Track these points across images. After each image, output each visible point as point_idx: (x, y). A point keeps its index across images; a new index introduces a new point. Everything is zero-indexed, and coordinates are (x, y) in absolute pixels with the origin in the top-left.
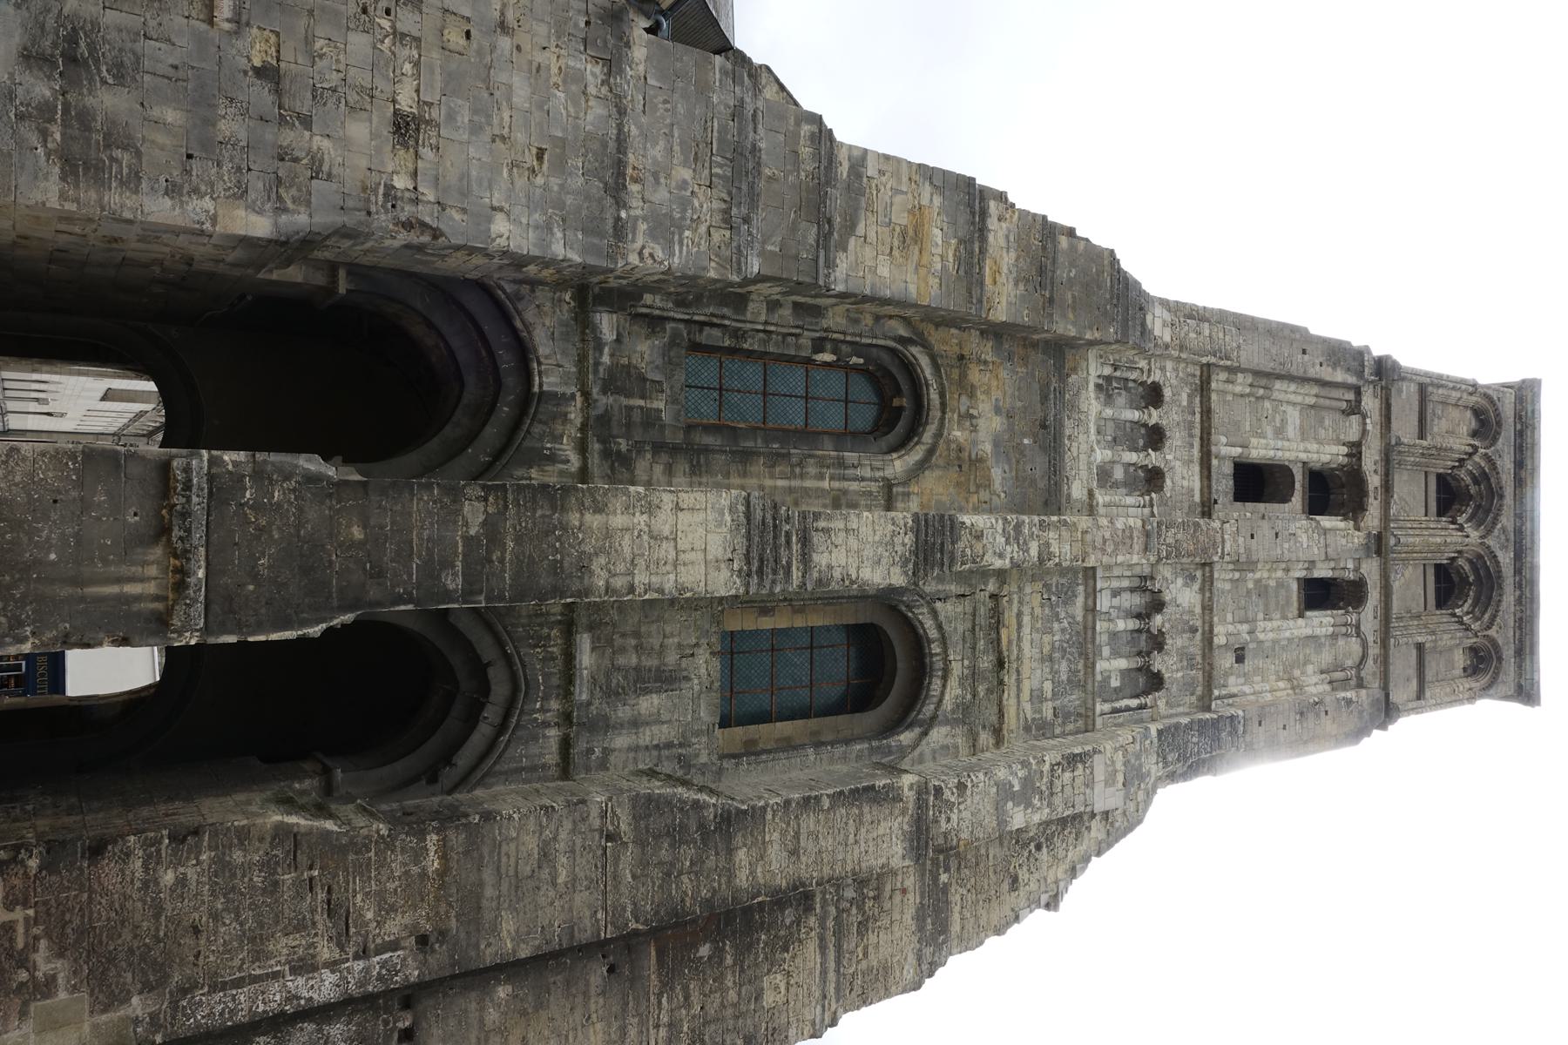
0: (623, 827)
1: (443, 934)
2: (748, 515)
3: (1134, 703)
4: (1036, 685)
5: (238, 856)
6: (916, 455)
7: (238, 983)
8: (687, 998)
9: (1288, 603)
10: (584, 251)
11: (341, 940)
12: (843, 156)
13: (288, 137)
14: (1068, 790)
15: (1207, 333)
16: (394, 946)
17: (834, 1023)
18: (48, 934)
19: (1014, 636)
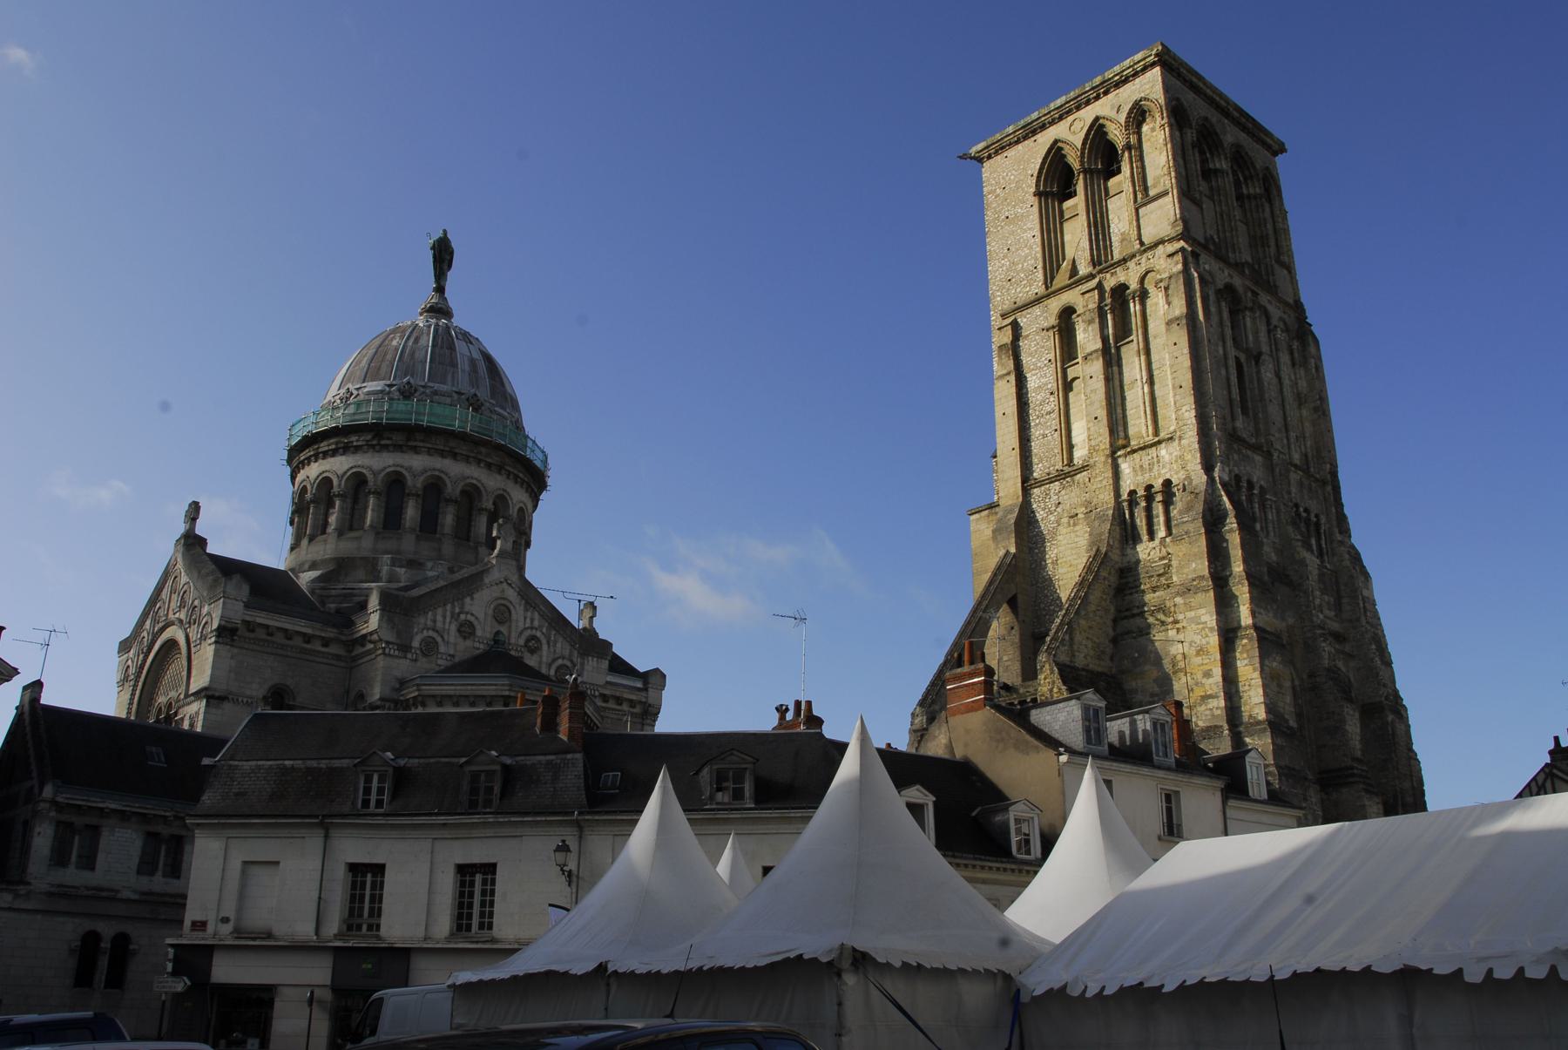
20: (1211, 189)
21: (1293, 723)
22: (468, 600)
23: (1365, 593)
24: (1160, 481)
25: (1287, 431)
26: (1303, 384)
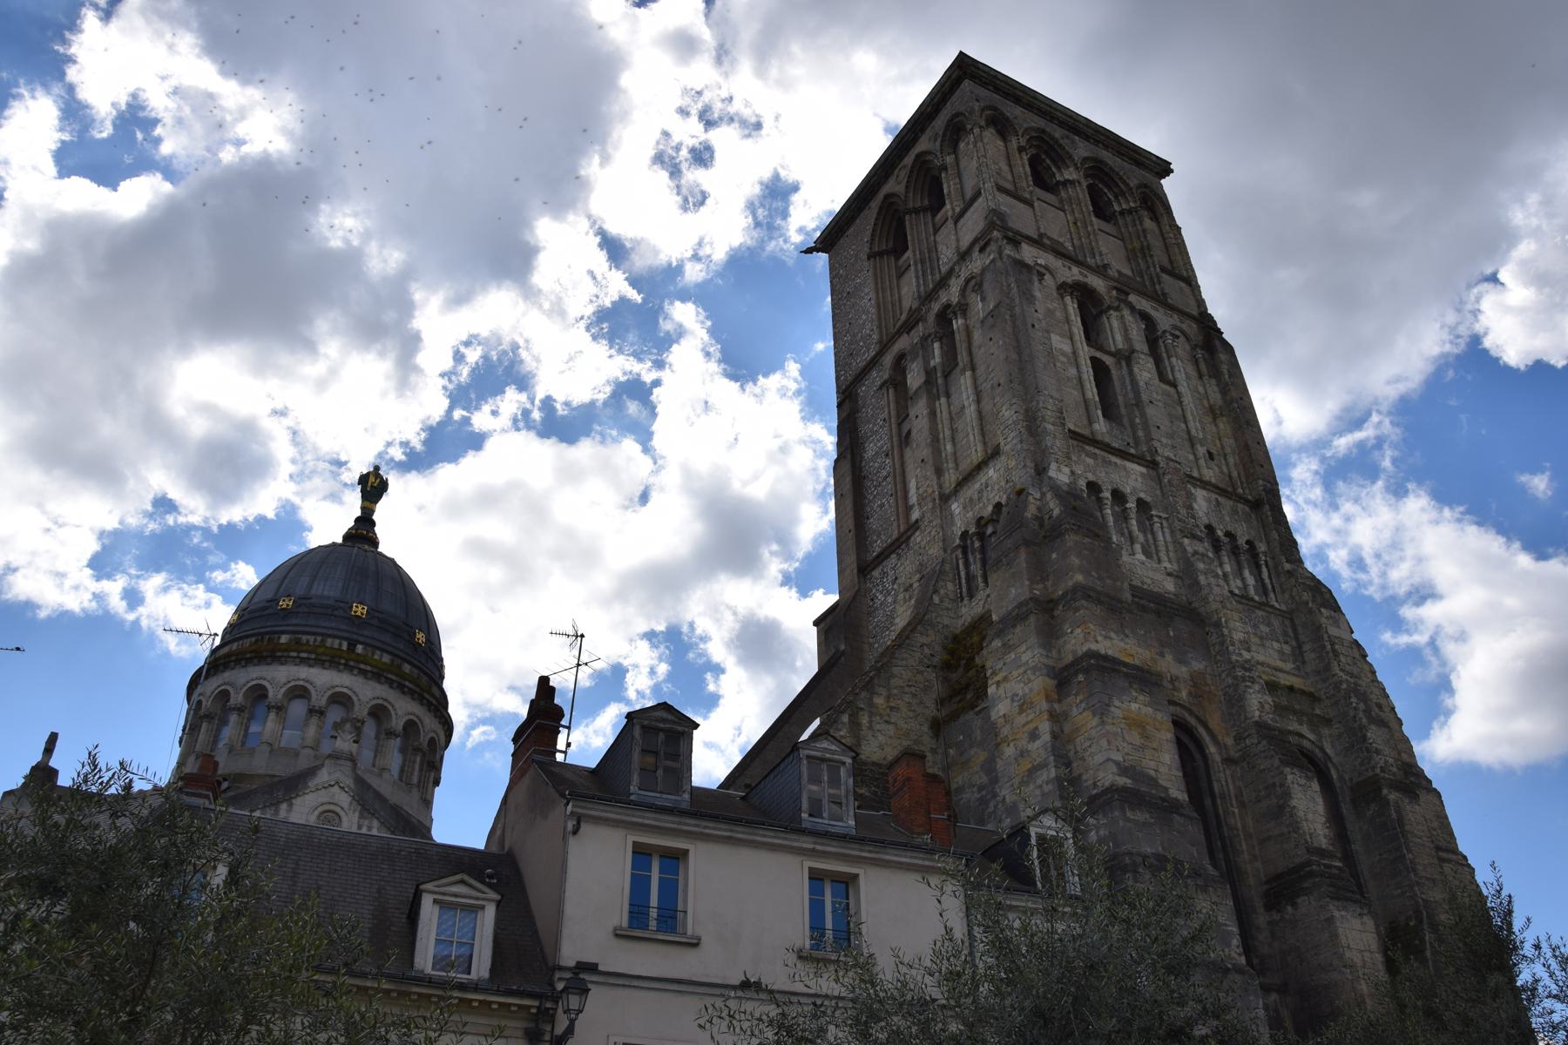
2: (1338, 899)
3: (1264, 569)
4: (1276, 655)
6: (1201, 730)
9: (1169, 395)
15: (1050, 427)
17: (1465, 858)
20: (1061, 201)
21: (1178, 792)
22: (284, 806)
23: (1333, 631)
24: (990, 508)
25: (1193, 446)
26: (1215, 397)
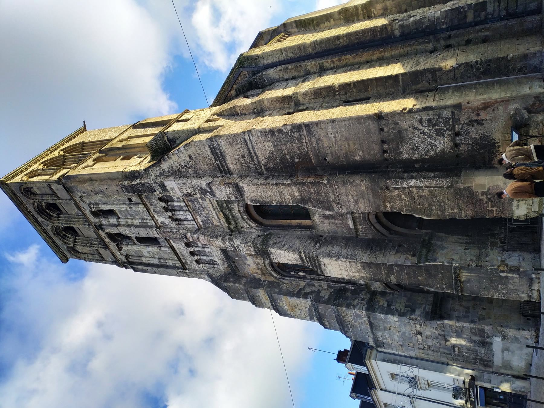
0: (335, 205)
1: (382, 189)
5: (439, 213)
7: (436, 187)
8: (299, 149)
10: (376, 315)
11: (410, 193)
12: (317, 320)
13: (443, 333)
14: (187, 188)
16: (395, 188)
18: (484, 204)
19: (219, 215)
